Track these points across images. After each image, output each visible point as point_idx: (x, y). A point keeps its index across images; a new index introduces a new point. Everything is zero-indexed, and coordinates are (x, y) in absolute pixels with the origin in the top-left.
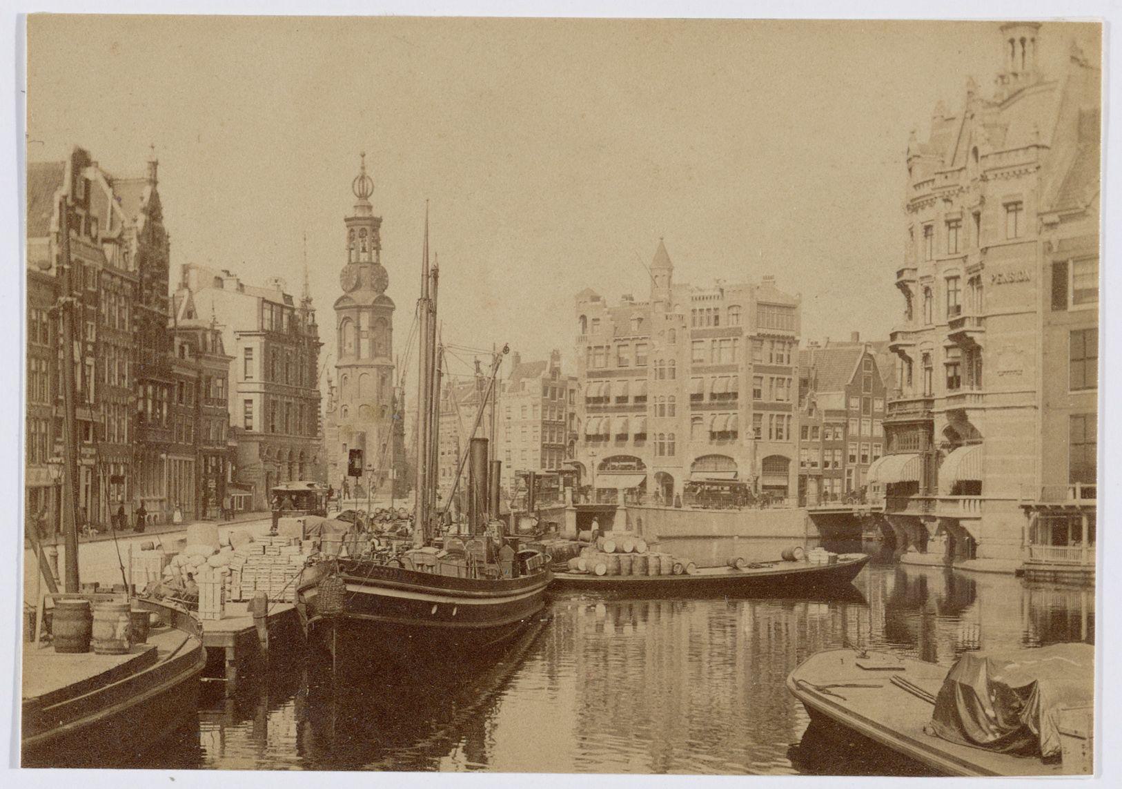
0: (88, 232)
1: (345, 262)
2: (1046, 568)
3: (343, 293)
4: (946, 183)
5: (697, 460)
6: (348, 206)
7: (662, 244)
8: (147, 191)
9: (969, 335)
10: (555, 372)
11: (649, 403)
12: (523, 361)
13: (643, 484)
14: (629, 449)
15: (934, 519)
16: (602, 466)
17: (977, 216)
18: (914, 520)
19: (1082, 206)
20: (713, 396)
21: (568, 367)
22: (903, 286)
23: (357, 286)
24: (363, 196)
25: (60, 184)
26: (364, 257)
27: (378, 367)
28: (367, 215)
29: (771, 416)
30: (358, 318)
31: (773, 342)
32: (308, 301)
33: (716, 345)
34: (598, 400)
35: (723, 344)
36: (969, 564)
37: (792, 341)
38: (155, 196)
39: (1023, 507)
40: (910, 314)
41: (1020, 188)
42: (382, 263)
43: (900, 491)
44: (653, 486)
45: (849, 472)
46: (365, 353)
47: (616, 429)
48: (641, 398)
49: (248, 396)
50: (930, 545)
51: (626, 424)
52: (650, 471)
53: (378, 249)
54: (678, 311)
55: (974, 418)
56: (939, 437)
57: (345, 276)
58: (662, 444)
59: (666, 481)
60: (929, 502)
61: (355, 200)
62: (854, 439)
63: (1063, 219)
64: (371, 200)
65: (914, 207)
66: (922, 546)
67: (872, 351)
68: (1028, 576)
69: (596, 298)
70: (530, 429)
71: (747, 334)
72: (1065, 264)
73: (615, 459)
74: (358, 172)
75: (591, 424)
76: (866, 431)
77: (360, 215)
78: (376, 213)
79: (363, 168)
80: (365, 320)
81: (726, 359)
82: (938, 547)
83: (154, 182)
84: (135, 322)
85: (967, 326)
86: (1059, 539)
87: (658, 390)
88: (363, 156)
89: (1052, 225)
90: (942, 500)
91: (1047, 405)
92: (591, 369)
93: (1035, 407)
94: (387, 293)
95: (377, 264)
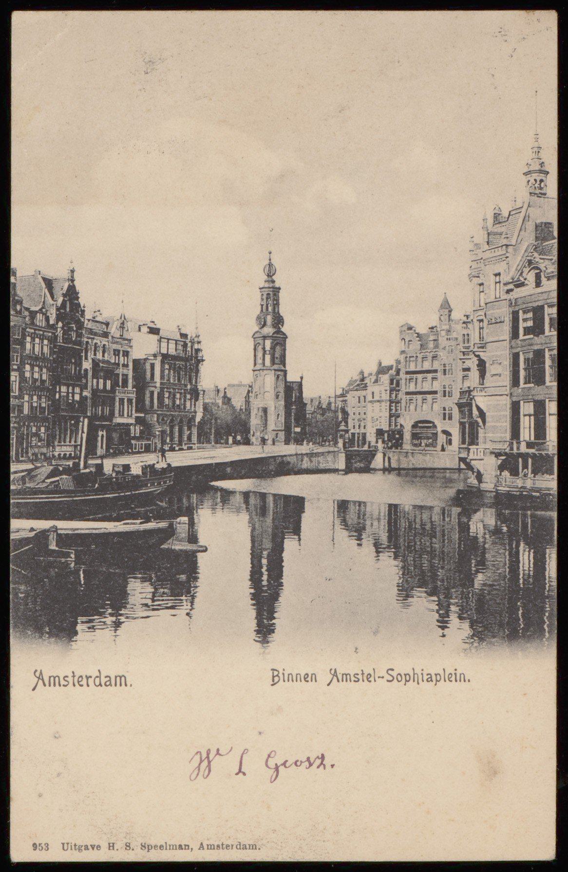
1: (258, 313)
3: (256, 328)
12: (383, 365)
23: (264, 325)
28: (271, 285)
39: (492, 453)
41: (501, 267)
54: (454, 335)
64: (274, 277)
74: (267, 262)
80: (268, 344)
88: (270, 253)
94: (283, 329)
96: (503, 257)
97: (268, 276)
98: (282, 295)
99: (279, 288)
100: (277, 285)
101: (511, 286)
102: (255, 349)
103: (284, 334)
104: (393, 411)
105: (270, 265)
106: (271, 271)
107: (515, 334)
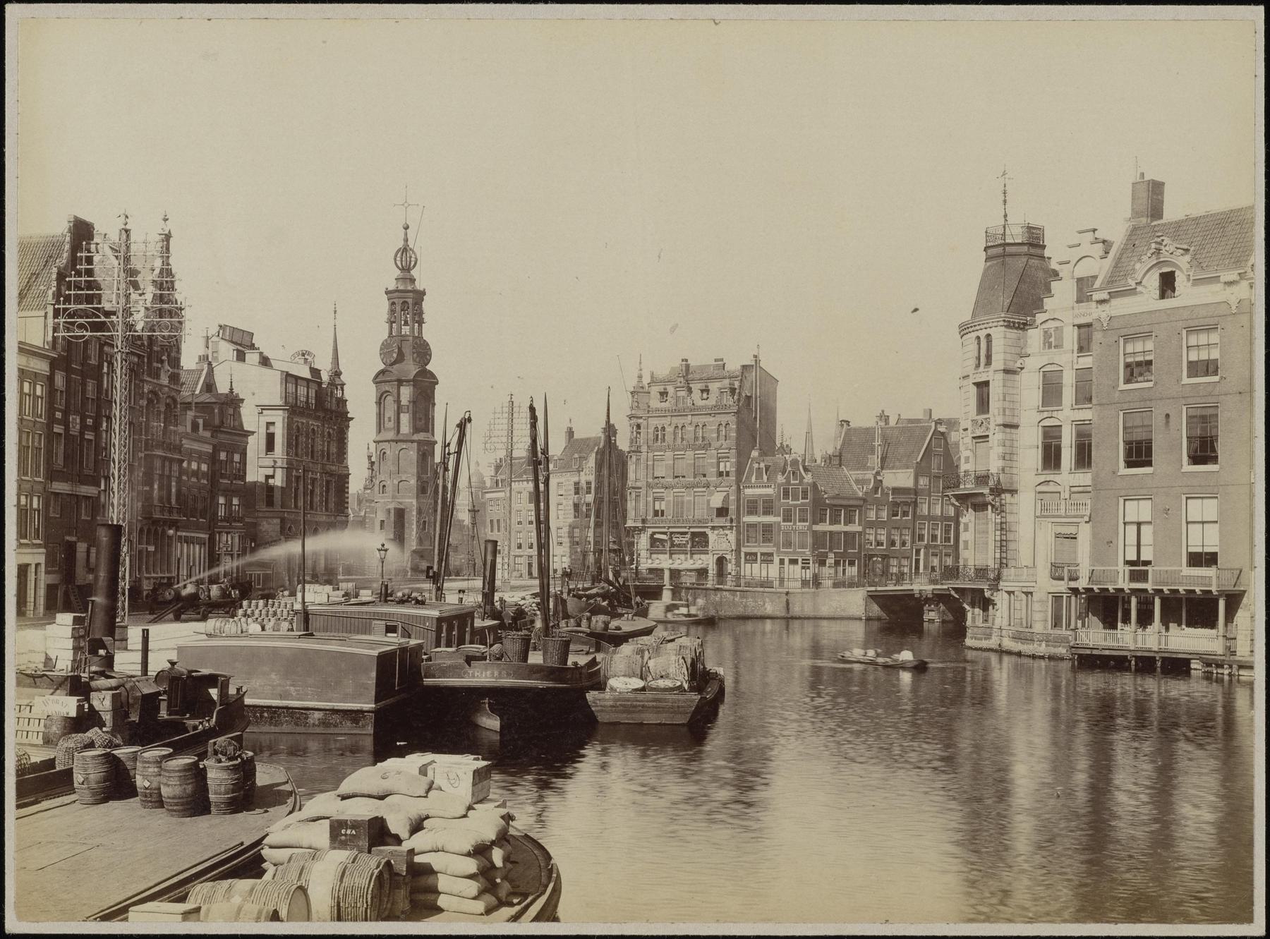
1: (386, 336)
3: (383, 367)
24: (406, 269)
26: (406, 330)
42: (427, 336)
46: (405, 428)
53: (421, 322)
62: (924, 518)
76: (937, 511)
77: (401, 288)
78: (419, 286)
79: (406, 240)
80: (406, 393)
88: (406, 228)
94: (428, 367)
95: (420, 337)
97: (402, 269)
98: (427, 305)
99: (423, 293)
102: (380, 402)
103: (432, 375)
106: (406, 260)
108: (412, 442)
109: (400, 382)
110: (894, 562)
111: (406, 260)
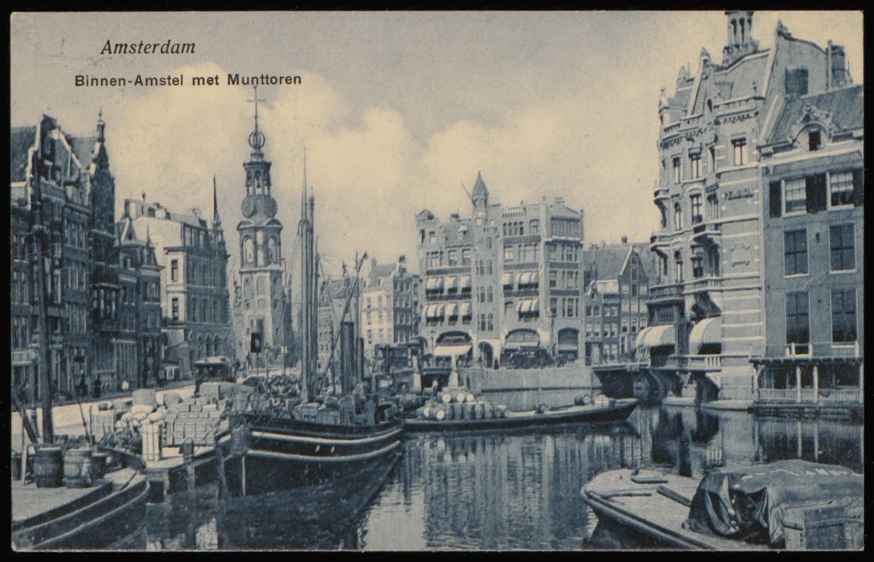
0: (54, 178)
2: (771, 405)
4: (688, 126)
5: (510, 333)
6: (246, 154)
7: (479, 175)
8: (97, 146)
9: (709, 237)
10: (403, 270)
11: (473, 292)
12: (379, 263)
13: (470, 352)
14: (459, 326)
15: (685, 372)
16: (439, 341)
17: (712, 151)
18: (671, 374)
19: (790, 141)
20: (520, 286)
21: (413, 268)
22: (658, 202)
23: (254, 212)
24: (257, 147)
25: (32, 143)
26: (259, 191)
27: (271, 272)
28: (260, 160)
29: (564, 300)
30: (255, 237)
31: (563, 246)
32: (218, 224)
33: (522, 248)
34: (435, 291)
35: (527, 248)
36: (715, 403)
37: (578, 245)
38: (103, 150)
40: (664, 222)
42: (273, 196)
43: (660, 352)
44: (477, 353)
45: (623, 340)
46: (261, 261)
47: (449, 312)
48: (467, 290)
49: (175, 295)
50: (684, 391)
51: (456, 308)
52: (476, 340)
53: (269, 184)
54: (493, 223)
55: (716, 299)
56: (689, 312)
57: (245, 206)
58: (483, 323)
59: (487, 349)
60: (683, 360)
61: (252, 150)
62: (626, 314)
63: (776, 150)
64: (263, 150)
65: (665, 144)
66: (678, 392)
67: (637, 250)
68: (757, 412)
69: (431, 217)
70: (385, 314)
71: (544, 239)
72: (822, 176)
73: (449, 334)
74: (253, 129)
75: (431, 310)
76: (635, 309)
77: (255, 160)
79: (257, 126)
80: (260, 235)
81: (529, 259)
82: (689, 394)
83: (101, 140)
84: (90, 243)
85: (707, 231)
86: (780, 384)
87: (477, 283)
88: (256, 117)
89: (768, 155)
90: (693, 359)
91: (768, 287)
92: (429, 268)
93: (760, 289)
94: (276, 217)
95: (269, 195)
96: (752, 114)
98: (273, 171)
100: (267, 159)
101: (770, 150)
103: (279, 223)
104: (398, 322)
105: (256, 134)
106: (257, 141)
107: (774, 208)
108: (265, 271)
109: (256, 229)
110: (606, 347)
111: (257, 141)
